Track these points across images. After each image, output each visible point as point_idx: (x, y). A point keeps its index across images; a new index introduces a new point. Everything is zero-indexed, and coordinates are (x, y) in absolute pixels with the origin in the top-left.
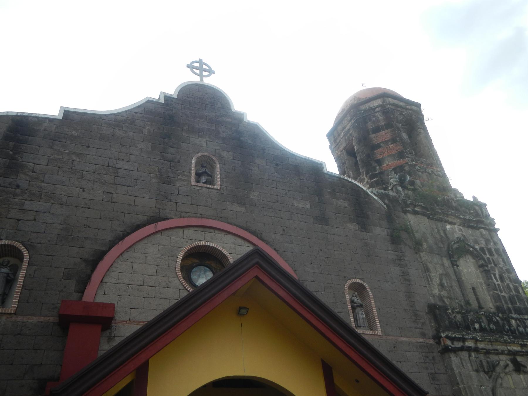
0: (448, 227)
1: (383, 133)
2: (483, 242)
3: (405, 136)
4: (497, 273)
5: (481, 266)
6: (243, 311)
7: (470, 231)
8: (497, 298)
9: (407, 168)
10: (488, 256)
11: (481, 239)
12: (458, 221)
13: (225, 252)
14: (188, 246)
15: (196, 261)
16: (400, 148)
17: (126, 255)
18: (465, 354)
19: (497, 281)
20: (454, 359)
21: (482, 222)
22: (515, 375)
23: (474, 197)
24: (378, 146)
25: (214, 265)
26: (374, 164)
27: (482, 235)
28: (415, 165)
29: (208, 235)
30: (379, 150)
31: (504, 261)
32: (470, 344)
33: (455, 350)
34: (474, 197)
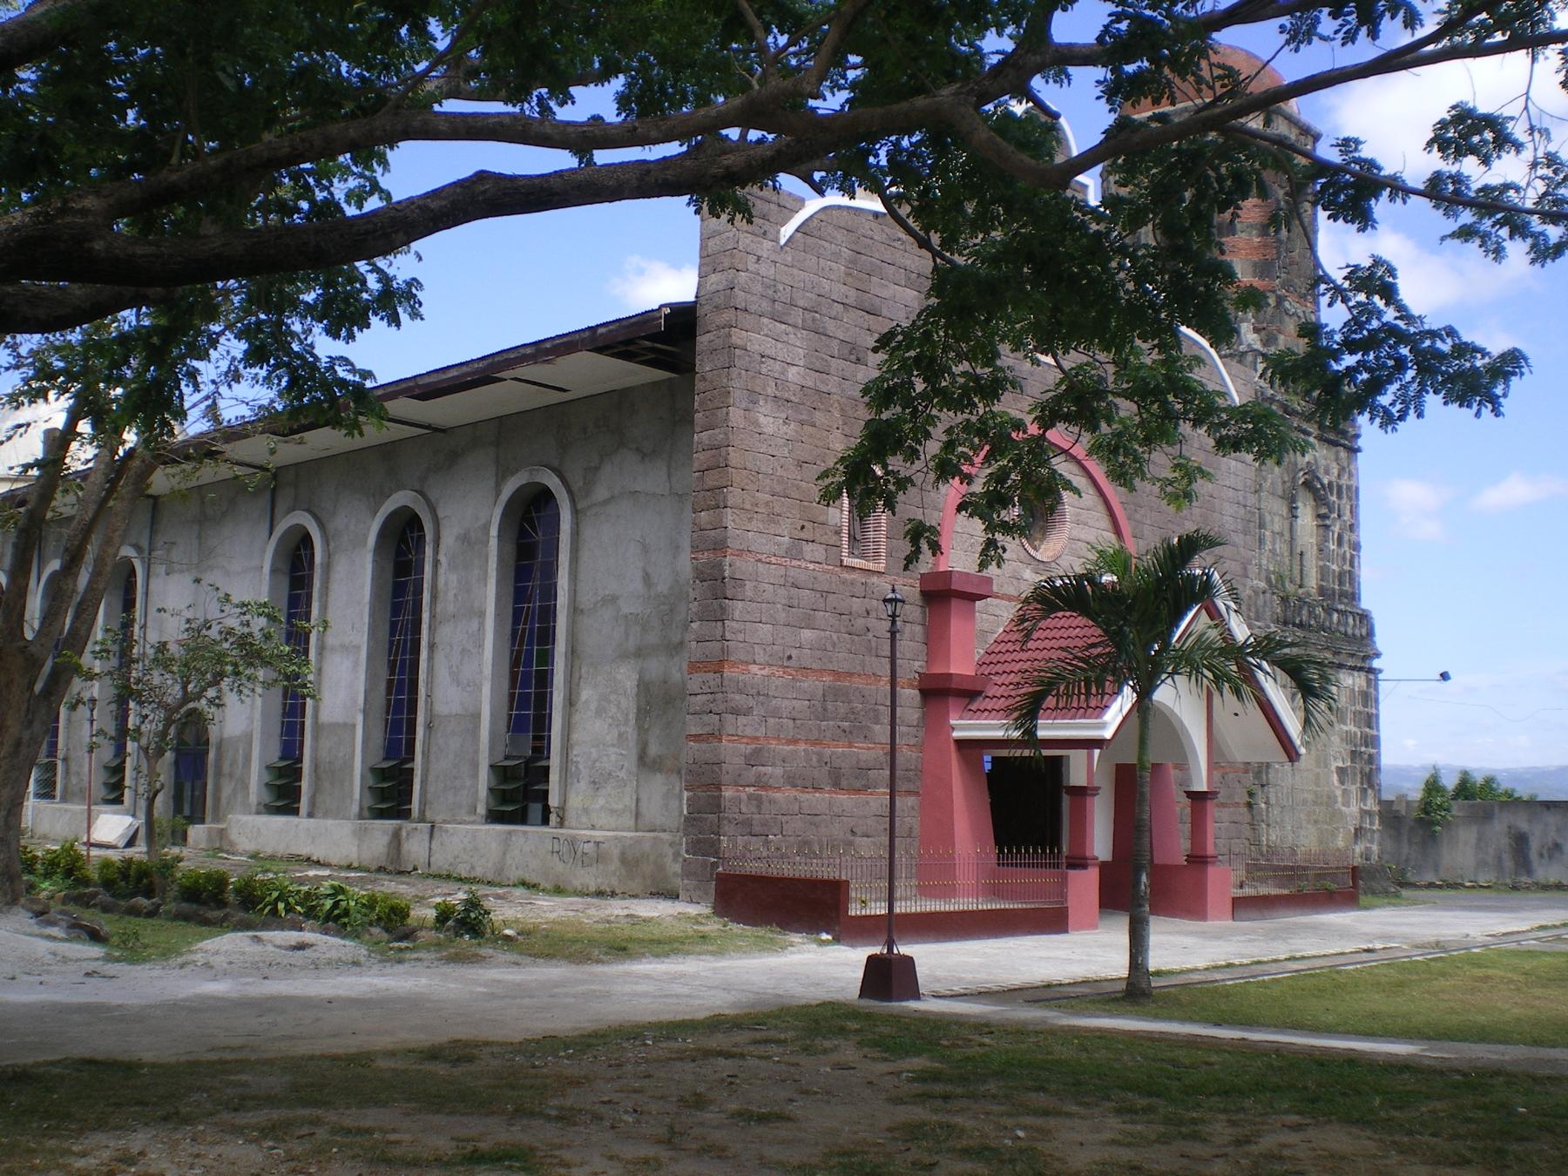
4: (1337, 529)
8: (1323, 572)
11: (1334, 465)
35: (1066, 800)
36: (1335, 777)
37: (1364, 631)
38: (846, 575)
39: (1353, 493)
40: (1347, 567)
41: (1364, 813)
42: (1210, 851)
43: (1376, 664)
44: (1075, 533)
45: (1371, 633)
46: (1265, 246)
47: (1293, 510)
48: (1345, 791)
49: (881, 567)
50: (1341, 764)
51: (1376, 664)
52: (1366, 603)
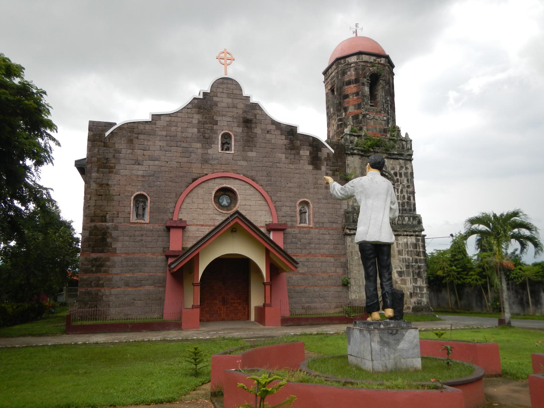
1: (352, 86)
2: (398, 168)
3: (367, 89)
4: (400, 188)
6: (234, 230)
7: (392, 161)
9: (360, 117)
10: (398, 177)
13: (235, 190)
14: (217, 188)
15: (222, 193)
17: (189, 195)
19: (398, 193)
21: (402, 155)
23: (407, 134)
24: (347, 96)
25: (231, 194)
26: (343, 111)
28: (367, 114)
29: (227, 181)
30: (347, 100)
31: (408, 180)
34: (407, 134)
37: (415, 222)
38: (132, 225)
40: (406, 200)
41: (415, 288)
43: (423, 233)
44: (244, 203)
45: (420, 222)
46: (358, 99)
48: (402, 280)
49: (148, 222)
50: (400, 270)
51: (423, 233)
52: (418, 212)
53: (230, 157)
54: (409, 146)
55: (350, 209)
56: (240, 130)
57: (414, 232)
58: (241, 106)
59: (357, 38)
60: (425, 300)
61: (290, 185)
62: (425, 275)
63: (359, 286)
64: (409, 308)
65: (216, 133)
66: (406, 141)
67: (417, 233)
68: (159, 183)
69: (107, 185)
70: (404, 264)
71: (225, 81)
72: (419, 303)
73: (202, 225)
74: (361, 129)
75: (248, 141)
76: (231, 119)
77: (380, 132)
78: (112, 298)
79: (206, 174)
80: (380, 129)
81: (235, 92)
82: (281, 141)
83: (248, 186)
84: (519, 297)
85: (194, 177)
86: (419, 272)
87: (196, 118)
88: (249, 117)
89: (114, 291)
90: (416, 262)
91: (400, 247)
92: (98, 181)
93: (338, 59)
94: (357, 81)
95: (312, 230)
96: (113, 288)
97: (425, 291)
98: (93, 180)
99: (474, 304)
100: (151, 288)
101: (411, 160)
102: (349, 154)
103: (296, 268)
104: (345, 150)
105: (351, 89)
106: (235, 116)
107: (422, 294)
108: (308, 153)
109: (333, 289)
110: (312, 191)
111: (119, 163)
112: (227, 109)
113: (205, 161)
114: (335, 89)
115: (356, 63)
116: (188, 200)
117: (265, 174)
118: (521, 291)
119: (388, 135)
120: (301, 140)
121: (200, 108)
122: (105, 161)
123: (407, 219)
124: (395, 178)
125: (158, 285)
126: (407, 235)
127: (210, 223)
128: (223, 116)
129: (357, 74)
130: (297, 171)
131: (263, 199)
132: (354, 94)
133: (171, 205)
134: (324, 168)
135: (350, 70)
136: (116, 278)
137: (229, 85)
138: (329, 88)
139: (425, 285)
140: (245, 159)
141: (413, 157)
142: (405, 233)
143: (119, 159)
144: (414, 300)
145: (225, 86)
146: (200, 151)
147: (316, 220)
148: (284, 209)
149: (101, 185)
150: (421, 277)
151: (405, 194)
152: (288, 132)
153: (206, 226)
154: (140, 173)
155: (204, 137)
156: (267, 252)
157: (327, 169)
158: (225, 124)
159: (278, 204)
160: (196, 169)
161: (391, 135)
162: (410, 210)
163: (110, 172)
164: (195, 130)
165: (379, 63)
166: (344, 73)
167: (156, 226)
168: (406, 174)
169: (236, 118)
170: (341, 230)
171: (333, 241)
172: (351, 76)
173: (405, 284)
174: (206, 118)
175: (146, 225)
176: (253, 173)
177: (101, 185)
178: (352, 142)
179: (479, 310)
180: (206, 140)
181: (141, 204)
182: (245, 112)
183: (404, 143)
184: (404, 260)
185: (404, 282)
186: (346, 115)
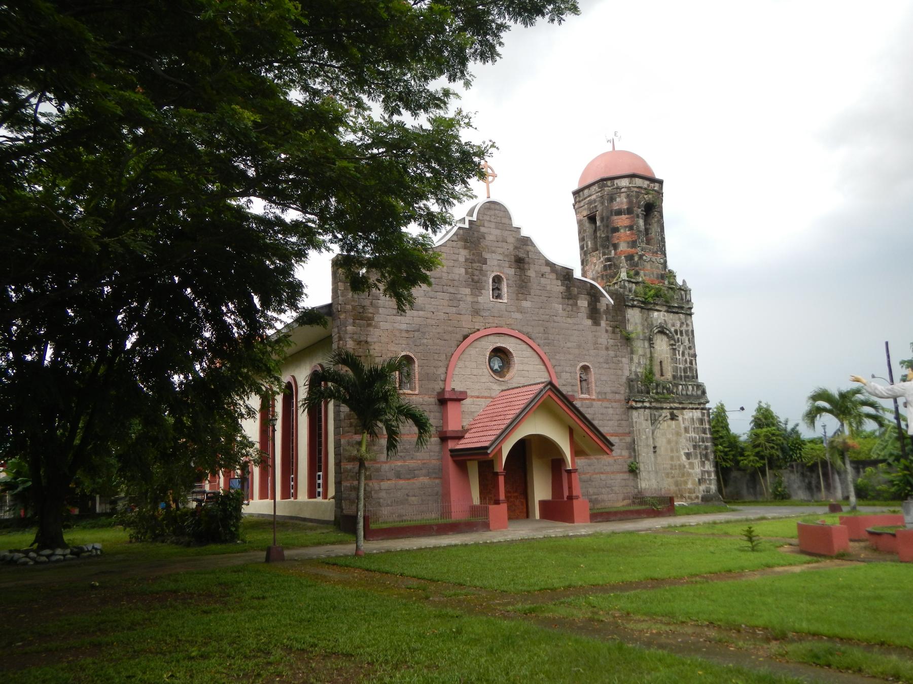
0: (656, 314)
3: (641, 222)
5: (672, 345)
7: (671, 315)
8: (675, 369)
9: (636, 259)
12: (665, 308)
14: (491, 348)
16: (635, 238)
18: (642, 410)
20: (635, 413)
21: (682, 308)
22: (670, 422)
23: (684, 281)
24: (616, 230)
26: (611, 248)
27: (680, 319)
29: (502, 338)
30: (616, 234)
32: (647, 405)
33: (636, 408)
34: (684, 281)
35: (565, 476)
36: (684, 458)
37: (699, 392)
39: (691, 334)
40: (688, 365)
41: (703, 472)
42: (574, 494)
43: (707, 406)
44: (521, 368)
45: (704, 392)
46: (632, 234)
47: (651, 345)
49: (417, 392)
51: (707, 406)
53: (503, 307)
54: (688, 297)
55: (633, 376)
56: (511, 271)
57: (699, 404)
58: (511, 240)
59: (615, 154)
60: (713, 487)
61: (569, 345)
62: (712, 457)
63: (649, 472)
64: (697, 497)
65: (486, 275)
66: (685, 291)
67: (702, 406)
68: (425, 341)
69: (366, 342)
70: (692, 444)
71: (492, 206)
72: (708, 491)
73: (478, 397)
74: (637, 274)
75: (521, 287)
76: (501, 257)
77: (658, 278)
78: (383, 494)
79: (478, 330)
80: (658, 274)
81: (504, 221)
82: (557, 287)
83: (525, 346)
84: (807, 481)
85: (465, 333)
86: (707, 453)
87: (463, 254)
88: (521, 255)
89: (385, 485)
90: (703, 442)
91: (687, 424)
92: (355, 337)
93: (603, 180)
94: (629, 211)
95: (594, 403)
96: (383, 480)
97: (713, 476)
98: (348, 336)
99: (744, 491)
100: (425, 480)
101: (691, 315)
102: (629, 306)
103: (612, 450)
104: (625, 301)
105: (622, 221)
106: (506, 253)
107: (710, 480)
108: (585, 304)
109: (620, 476)
110: (592, 352)
111: (378, 313)
112: (496, 244)
113: (476, 312)
114: (598, 218)
115: (628, 188)
116: (460, 364)
117: (542, 329)
118: (808, 474)
119: (666, 282)
120: (578, 287)
121: (466, 241)
122: (361, 310)
123: (690, 388)
124: (676, 337)
125: (434, 476)
126: (692, 409)
127: (486, 394)
128: (494, 252)
129: (630, 202)
130: (576, 327)
131: (541, 363)
132: (626, 227)
133: (443, 370)
134: (603, 323)
135: (620, 196)
136: (385, 467)
137: (497, 212)
138: (585, 213)
139: (712, 469)
140: (520, 310)
141: (693, 311)
142: (691, 406)
143: (377, 307)
144: (702, 487)
145: (492, 212)
146: (469, 299)
147: (598, 390)
148: (564, 375)
149: (359, 343)
150: (708, 460)
151: (687, 356)
152: (564, 276)
153: (482, 397)
154: (404, 327)
155: (473, 280)
156: (571, 432)
157: (607, 324)
158: (496, 263)
159: (558, 369)
160: (467, 323)
161: (669, 283)
162: (693, 377)
163: (369, 325)
164: (463, 271)
165: (653, 190)
166: (612, 199)
167: (426, 398)
168: (687, 331)
169: (507, 256)
170: (624, 402)
171: (617, 417)
172: (622, 203)
173: (693, 468)
174: (473, 254)
175: (414, 397)
176: (529, 329)
177: (359, 343)
178: (630, 291)
179: (752, 498)
180: (476, 285)
181: (406, 369)
182: (516, 248)
183: (683, 292)
184: (692, 439)
185: (692, 465)
186: (616, 254)
